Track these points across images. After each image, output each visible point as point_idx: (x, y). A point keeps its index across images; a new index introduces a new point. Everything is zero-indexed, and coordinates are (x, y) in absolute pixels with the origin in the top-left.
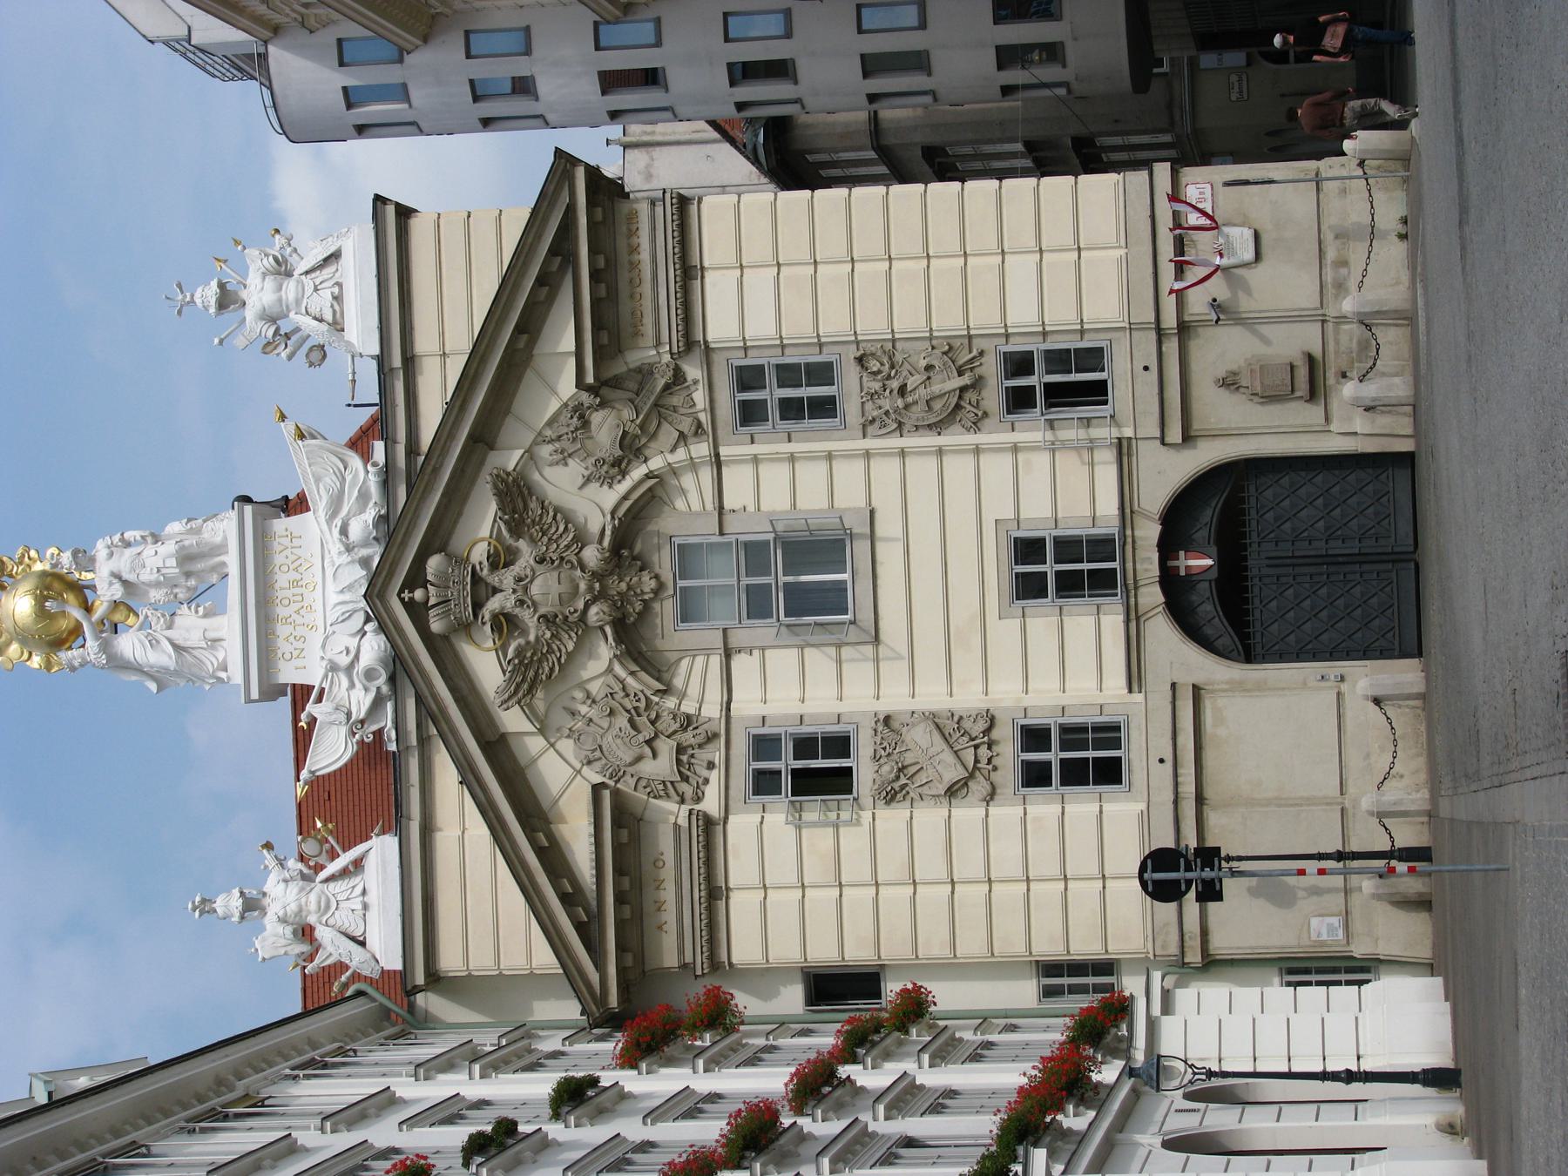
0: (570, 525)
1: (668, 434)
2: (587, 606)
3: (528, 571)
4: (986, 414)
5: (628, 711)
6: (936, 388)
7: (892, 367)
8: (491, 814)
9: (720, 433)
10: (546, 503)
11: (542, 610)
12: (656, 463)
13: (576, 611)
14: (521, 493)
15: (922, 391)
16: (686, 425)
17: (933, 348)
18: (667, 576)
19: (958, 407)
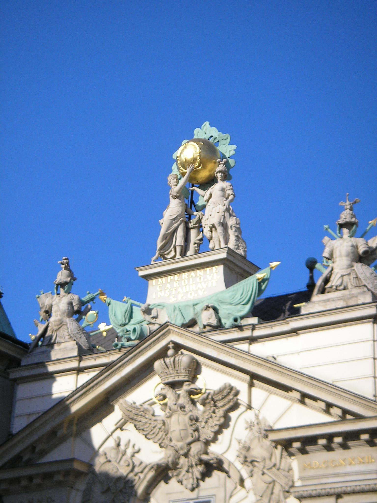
11: (167, 421)
12: (248, 483)
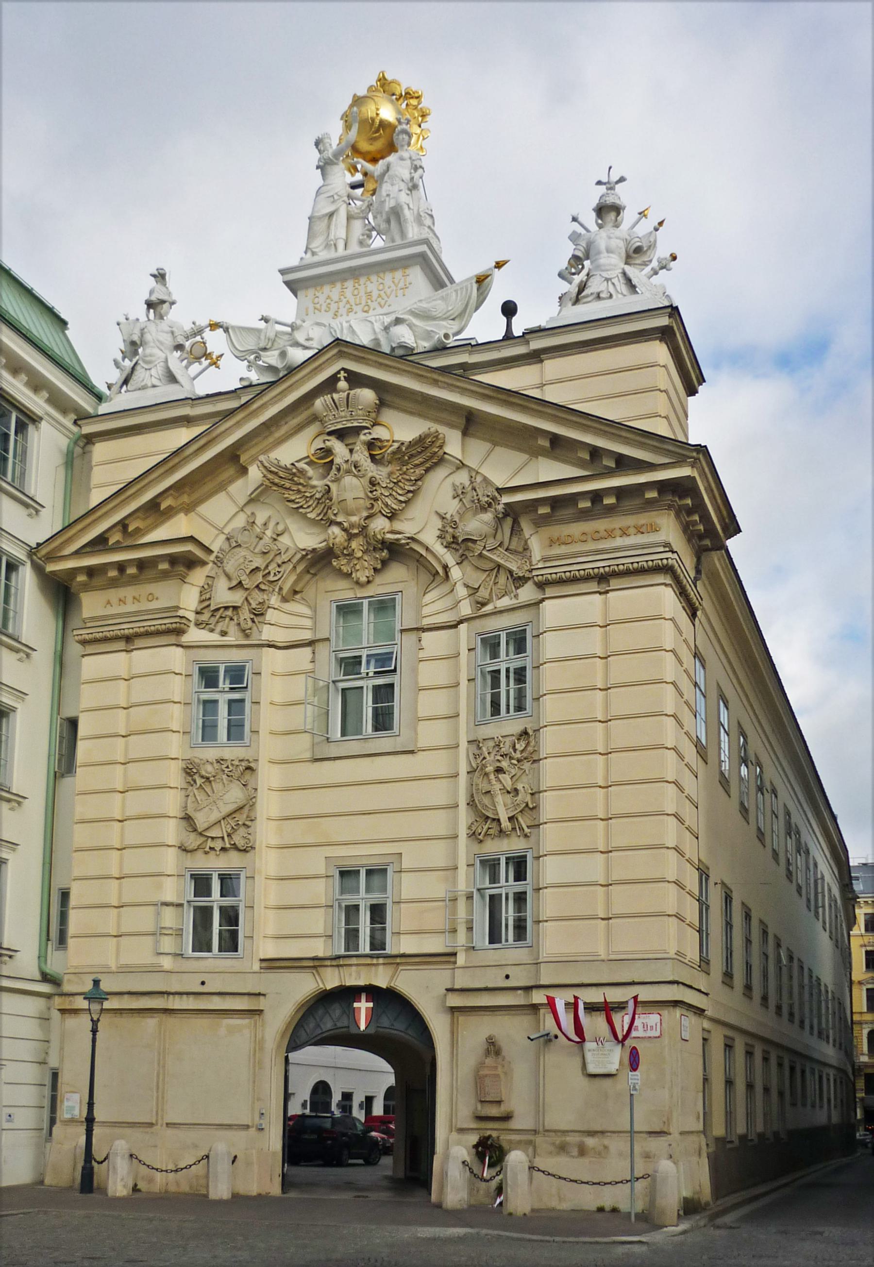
0: (404, 505)
1: (476, 578)
2: (339, 524)
3: (362, 472)
4: (481, 841)
5: (267, 566)
6: (500, 799)
7: (519, 761)
8: (176, 460)
9: (477, 622)
10: (420, 483)
11: (334, 487)
12: (456, 573)
13: (335, 515)
14: (426, 461)
15: (498, 786)
16: (483, 593)
17: (532, 794)
18: (370, 591)
19: (488, 818)
